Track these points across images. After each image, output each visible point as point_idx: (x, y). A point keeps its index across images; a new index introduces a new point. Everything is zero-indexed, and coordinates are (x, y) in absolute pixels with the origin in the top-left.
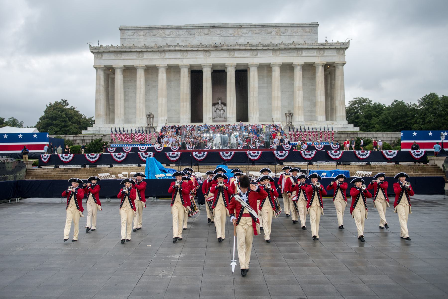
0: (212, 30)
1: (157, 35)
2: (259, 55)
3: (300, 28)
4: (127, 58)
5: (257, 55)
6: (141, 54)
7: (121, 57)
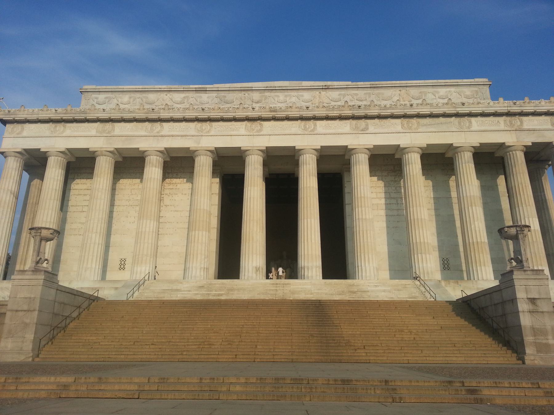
0: (267, 94)
1: (156, 104)
2: (371, 129)
3: (453, 89)
4: (76, 134)
5: (367, 128)
6: (108, 126)
7: (63, 132)
